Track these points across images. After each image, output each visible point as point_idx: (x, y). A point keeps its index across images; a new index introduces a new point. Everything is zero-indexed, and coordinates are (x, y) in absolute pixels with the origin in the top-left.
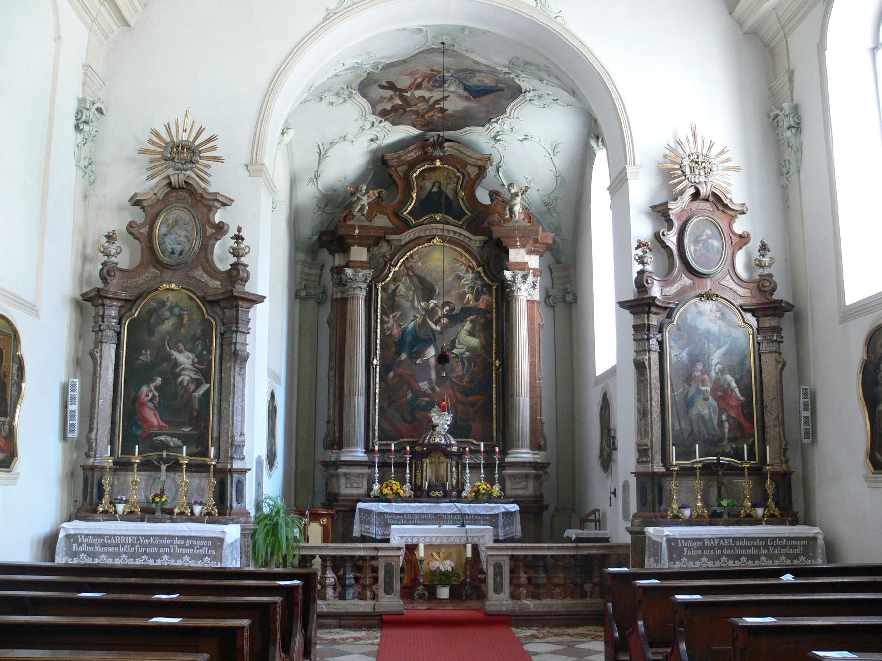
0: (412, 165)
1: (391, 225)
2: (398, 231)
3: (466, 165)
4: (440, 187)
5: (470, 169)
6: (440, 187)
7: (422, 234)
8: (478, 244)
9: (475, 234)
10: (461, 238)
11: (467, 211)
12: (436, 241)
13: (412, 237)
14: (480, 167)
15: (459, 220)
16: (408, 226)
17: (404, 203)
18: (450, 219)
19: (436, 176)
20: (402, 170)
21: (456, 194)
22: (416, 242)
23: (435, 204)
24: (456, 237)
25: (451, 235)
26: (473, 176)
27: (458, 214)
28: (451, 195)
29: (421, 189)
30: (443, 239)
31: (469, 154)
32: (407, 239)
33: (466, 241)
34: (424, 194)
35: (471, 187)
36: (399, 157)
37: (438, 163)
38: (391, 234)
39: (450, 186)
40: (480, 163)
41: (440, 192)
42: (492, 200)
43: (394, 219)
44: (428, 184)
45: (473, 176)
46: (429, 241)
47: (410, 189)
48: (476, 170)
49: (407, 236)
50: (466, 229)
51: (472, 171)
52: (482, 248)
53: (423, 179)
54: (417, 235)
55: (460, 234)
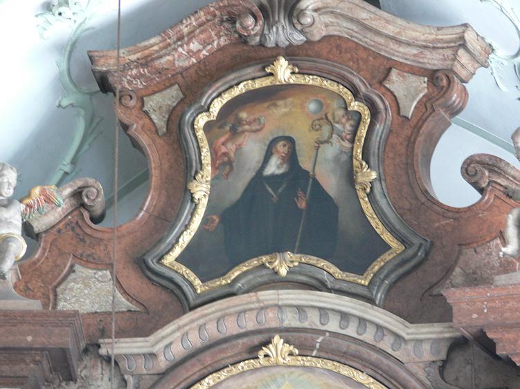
0: (195, 85)
1: (124, 303)
2: (143, 322)
3: (383, 69)
4: (292, 158)
5: (397, 83)
6: (292, 158)
7: (231, 327)
8: (427, 353)
9: (412, 317)
10: (369, 336)
11: (387, 237)
12: (279, 348)
13: (195, 340)
14: (432, 76)
15: (361, 271)
16: (182, 303)
17: (166, 220)
18: (328, 269)
19: (277, 118)
20: (160, 103)
21: (350, 176)
22: (208, 358)
23: (283, 216)
24: (351, 331)
25: (333, 325)
26: (410, 109)
27: (357, 252)
28: (330, 182)
29: (224, 165)
30: (302, 342)
31: (390, 30)
32: (178, 351)
33: (386, 344)
34: (238, 185)
35: (410, 145)
36: (146, 62)
37: (283, 71)
38: (122, 333)
39: (329, 151)
40: (433, 60)
41: (297, 176)
42: (482, 191)
43: (134, 280)
44: (252, 148)
45: (410, 109)
46: (252, 352)
47: (185, 169)
48: (421, 86)
49: (176, 338)
50: (387, 306)
51: (408, 90)
52: (443, 366)
53: (234, 133)
54: (212, 332)
55: (362, 321)
